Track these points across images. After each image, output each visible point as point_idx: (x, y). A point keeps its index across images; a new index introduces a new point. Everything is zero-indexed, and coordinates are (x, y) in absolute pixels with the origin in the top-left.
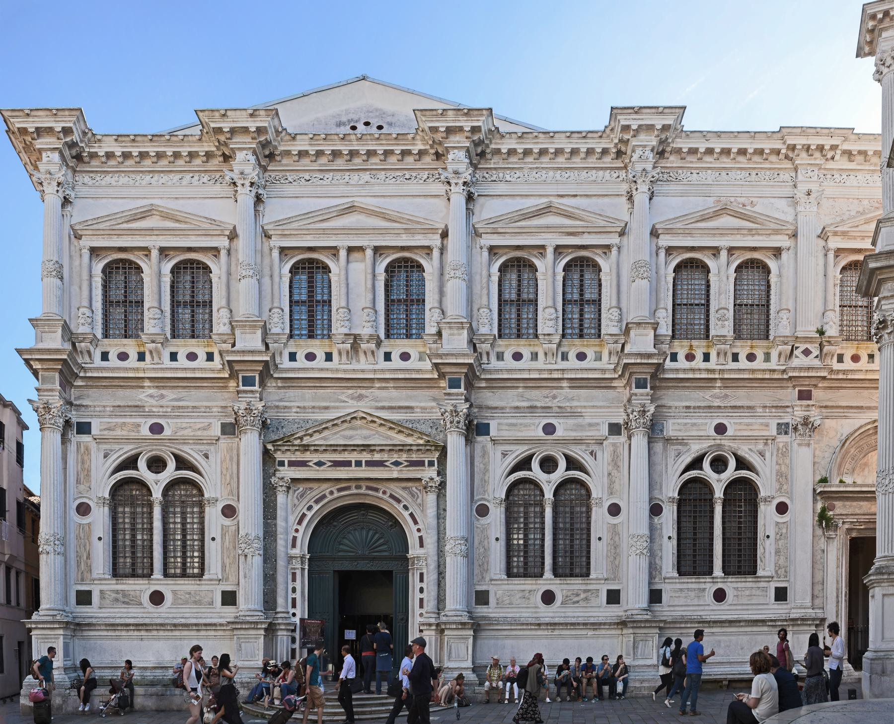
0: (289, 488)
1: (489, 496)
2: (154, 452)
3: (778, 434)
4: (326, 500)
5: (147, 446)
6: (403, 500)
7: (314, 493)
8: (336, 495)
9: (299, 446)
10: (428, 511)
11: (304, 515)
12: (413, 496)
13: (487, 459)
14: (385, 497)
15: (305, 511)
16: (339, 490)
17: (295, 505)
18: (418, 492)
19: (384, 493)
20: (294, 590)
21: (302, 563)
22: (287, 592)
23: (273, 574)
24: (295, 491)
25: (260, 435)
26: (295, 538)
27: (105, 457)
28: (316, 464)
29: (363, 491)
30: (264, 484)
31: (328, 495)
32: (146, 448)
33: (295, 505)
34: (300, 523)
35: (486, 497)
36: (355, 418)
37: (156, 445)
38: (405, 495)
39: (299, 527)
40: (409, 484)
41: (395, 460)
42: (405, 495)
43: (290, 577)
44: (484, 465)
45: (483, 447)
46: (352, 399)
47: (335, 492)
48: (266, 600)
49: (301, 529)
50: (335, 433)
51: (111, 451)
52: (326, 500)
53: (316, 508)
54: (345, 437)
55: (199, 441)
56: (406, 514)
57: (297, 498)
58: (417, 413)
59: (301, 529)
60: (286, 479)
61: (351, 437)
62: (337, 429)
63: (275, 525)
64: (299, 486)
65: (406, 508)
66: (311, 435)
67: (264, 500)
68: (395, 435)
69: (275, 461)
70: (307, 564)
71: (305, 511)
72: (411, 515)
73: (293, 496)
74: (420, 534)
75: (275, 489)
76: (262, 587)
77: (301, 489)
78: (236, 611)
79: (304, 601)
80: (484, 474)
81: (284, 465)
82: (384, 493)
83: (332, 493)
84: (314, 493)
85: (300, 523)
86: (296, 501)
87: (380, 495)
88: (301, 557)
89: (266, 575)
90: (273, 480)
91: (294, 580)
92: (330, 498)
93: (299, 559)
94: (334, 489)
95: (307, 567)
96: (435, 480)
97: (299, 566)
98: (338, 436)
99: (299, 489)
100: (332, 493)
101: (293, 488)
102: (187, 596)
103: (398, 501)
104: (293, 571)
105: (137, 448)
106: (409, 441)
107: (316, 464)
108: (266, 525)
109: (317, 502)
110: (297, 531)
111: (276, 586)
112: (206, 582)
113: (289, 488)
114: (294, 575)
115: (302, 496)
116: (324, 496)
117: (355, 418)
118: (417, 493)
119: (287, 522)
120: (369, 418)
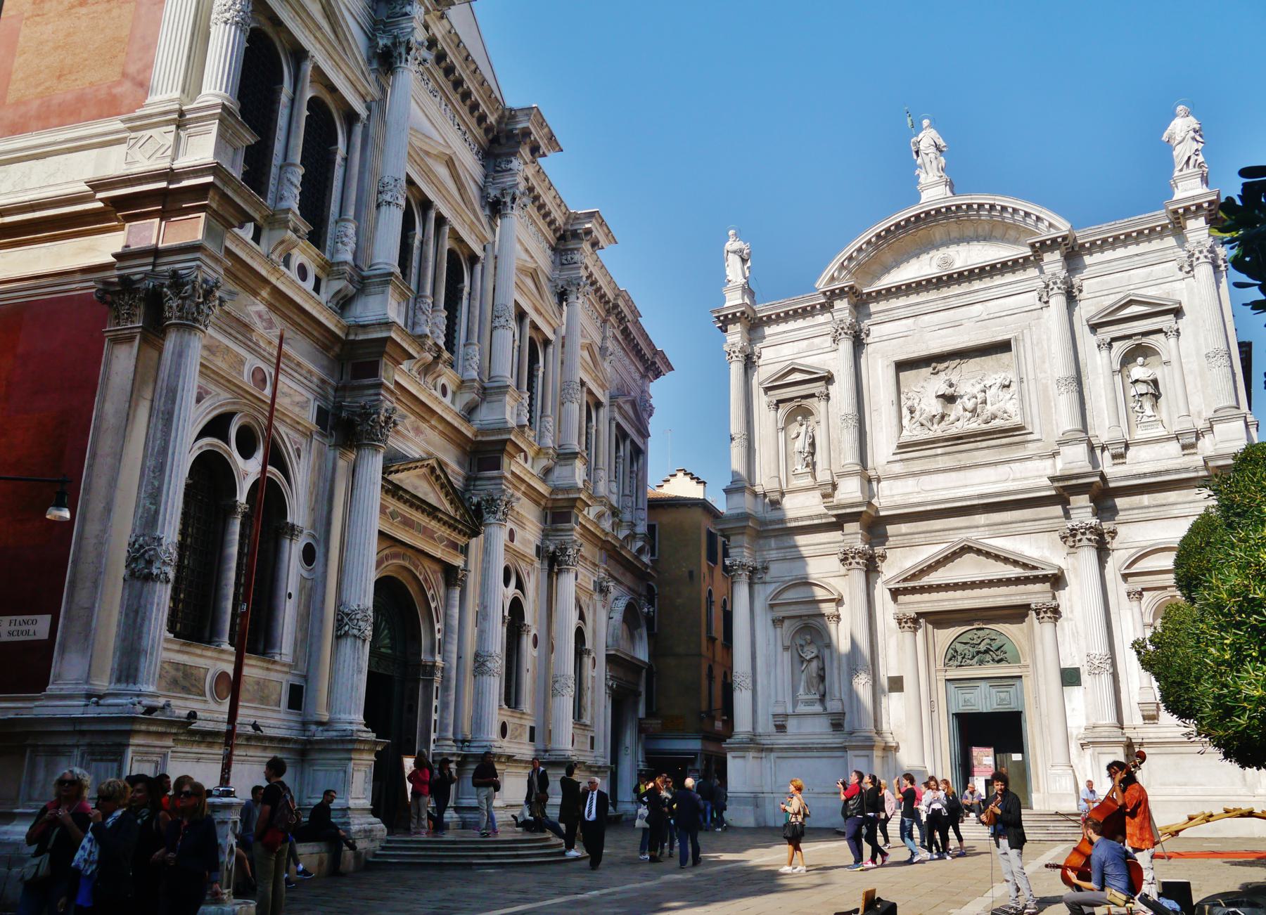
2: (248, 420)
3: (595, 590)
5: (245, 405)
14: (421, 578)
27: (198, 401)
32: (246, 408)
37: (254, 409)
40: (436, 567)
51: (207, 393)
55: (296, 426)
56: (433, 605)
61: (416, 488)
78: (299, 719)
102: (256, 687)
105: (234, 403)
112: (278, 668)
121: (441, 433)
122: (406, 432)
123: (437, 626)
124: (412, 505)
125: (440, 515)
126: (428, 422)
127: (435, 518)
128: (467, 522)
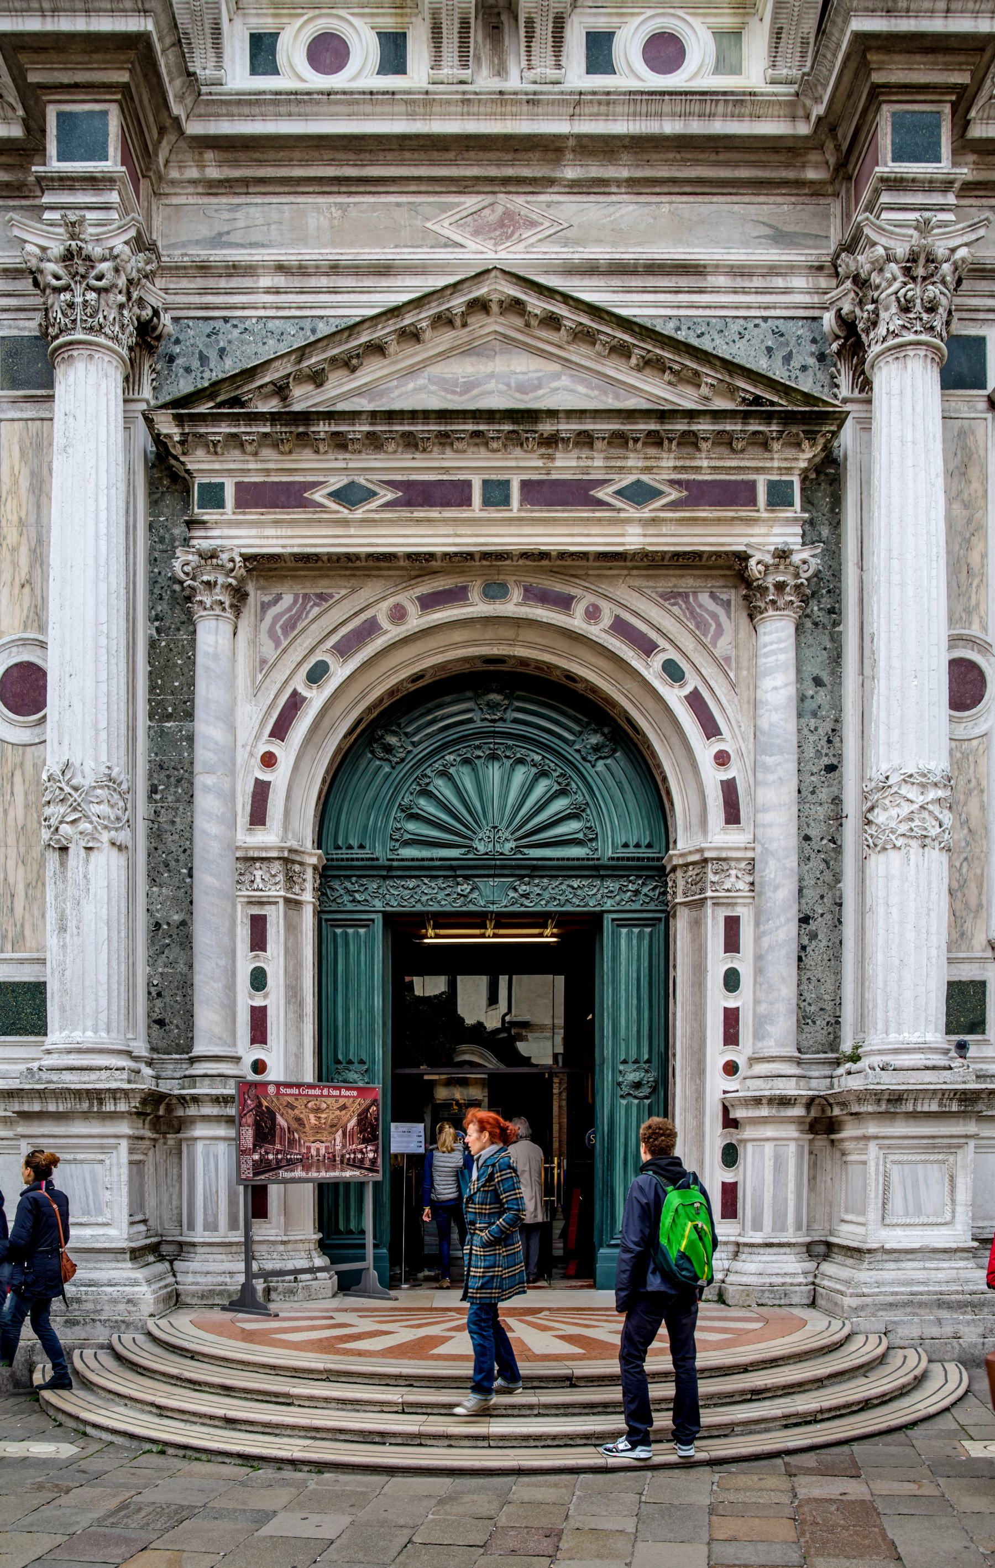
0: (239, 595)
1: (985, 629)
4: (378, 643)
6: (662, 642)
7: (336, 616)
8: (416, 621)
9: (274, 418)
10: (767, 683)
11: (295, 704)
12: (701, 625)
13: (975, 485)
14: (596, 631)
15: (299, 683)
16: (428, 602)
17: (263, 662)
18: (721, 612)
19: (593, 614)
20: (259, 980)
21: (290, 880)
22: (231, 987)
23: (183, 923)
24: (264, 607)
25: (130, 381)
26: (261, 791)
28: (336, 495)
29: (512, 606)
30: (153, 582)
31: (384, 623)
33: (263, 662)
34: (280, 731)
35: (975, 630)
36: (480, 306)
38: (668, 624)
39: (276, 748)
40: (687, 582)
41: (629, 479)
42: (668, 624)
43: (243, 933)
44: (966, 506)
45: (962, 434)
46: (476, 233)
47: (413, 610)
48: (155, 1016)
49: (286, 753)
50: (412, 372)
52: (378, 643)
53: (340, 672)
54: (446, 385)
56: (674, 696)
57: (272, 634)
58: (716, 290)
59: (286, 753)
60: (225, 556)
62: (412, 355)
63: (190, 739)
64: (276, 591)
65: (673, 672)
66: (317, 378)
67: (153, 644)
68: (633, 379)
69: (187, 490)
70: (309, 886)
71: (299, 683)
72: (695, 700)
73: (256, 628)
74: (726, 775)
75: (189, 599)
76: (142, 970)
77: (287, 600)
79: (301, 1017)
80: (967, 544)
81: (220, 504)
82: (593, 614)
83: (398, 615)
84: (336, 616)
85: (280, 731)
86: (269, 650)
87: (576, 621)
88: (286, 860)
89: (158, 925)
90: (182, 562)
91: (258, 942)
92: (393, 633)
93: (276, 867)
94: (407, 598)
95: (308, 896)
96: (796, 558)
97: (277, 891)
98: (421, 381)
99: (278, 598)
100: (398, 615)
101: (255, 596)
103: (648, 648)
104: (256, 911)
106: (686, 399)
107: (336, 495)
108: (159, 738)
109: (344, 650)
110: (269, 760)
111: (191, 967)
113: (239, 595)
114: (258, 926)
115: (290, 626)
116: (371, 628)
117: (480, 306)
118: (715, 616)
119: (232, 729)
120: (536, 305)
121: (635, 186)
122: (443, 254)
123: (705, 751)
124: (411, 442)
125: (566, 427)
126: (551, 182)
127: (552, 441)
128: (757, 400)
